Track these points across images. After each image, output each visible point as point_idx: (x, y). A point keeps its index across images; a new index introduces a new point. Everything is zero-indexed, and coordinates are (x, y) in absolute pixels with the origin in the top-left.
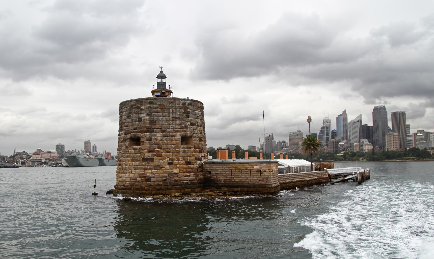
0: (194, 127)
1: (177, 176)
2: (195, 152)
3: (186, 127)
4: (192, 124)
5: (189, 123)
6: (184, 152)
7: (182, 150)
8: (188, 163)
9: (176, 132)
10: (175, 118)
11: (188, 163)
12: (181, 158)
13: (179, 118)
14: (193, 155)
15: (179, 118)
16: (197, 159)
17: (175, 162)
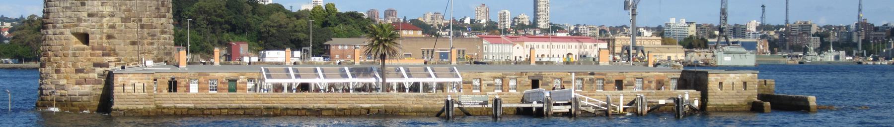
0: (95, 19)
1: (63, 89)
2: (91, 55)
3: (80, 20)
4: (90, 15)
5: (85, 14)
6: (74, 55)
7: (70, 52)
8: (78, 71)
9: (65, 27)
10: (67, 8)
11: (78, 71)
12: (69, 64)
13: (70, 8)
14: (89, 60)
15: (70, 8)
16: (96, 65)
17: (63, 69)
